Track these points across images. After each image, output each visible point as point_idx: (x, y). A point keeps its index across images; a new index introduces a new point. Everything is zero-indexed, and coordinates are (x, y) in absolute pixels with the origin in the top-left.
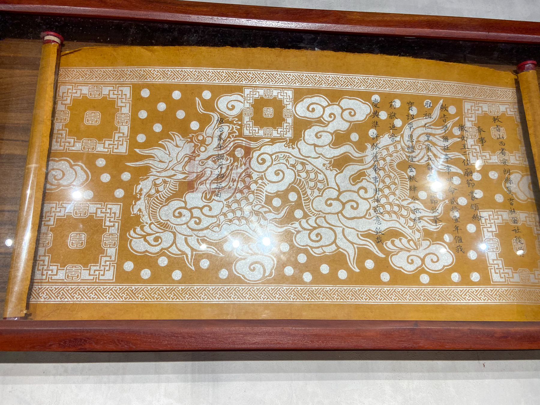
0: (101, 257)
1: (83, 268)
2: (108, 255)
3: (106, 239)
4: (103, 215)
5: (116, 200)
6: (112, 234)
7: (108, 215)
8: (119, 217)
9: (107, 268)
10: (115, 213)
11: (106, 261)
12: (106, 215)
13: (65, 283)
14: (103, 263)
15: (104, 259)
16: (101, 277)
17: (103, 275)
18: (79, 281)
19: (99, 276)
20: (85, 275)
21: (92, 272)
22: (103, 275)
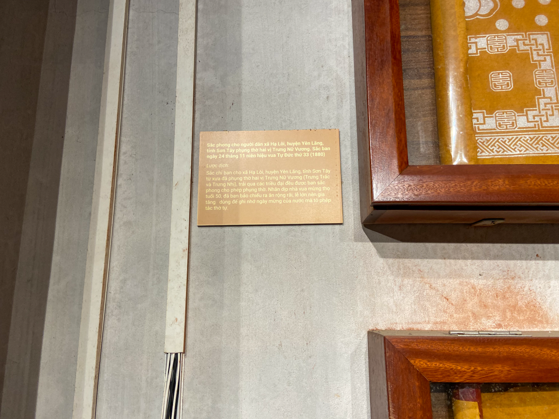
0: (538, 99)
1: (517, 114)
2: (546, 96)
3: (537, 77)
4: (527, 47)
5: (541, 29)
6: (546, 70)
7: (534, 47)
8: (549, 49)
9: (550, 112)
10: (542, 45)
11: (546, 104)
12: (531, 48)
13: (497, 133)
14: (542, 107)
15: (542, 101)
16: (545, 124)
17: (547, 121)
18: (516, 129)
19: (541, 123)
20: (522, 122)
21: (531, 118)
22: (547, 121)
